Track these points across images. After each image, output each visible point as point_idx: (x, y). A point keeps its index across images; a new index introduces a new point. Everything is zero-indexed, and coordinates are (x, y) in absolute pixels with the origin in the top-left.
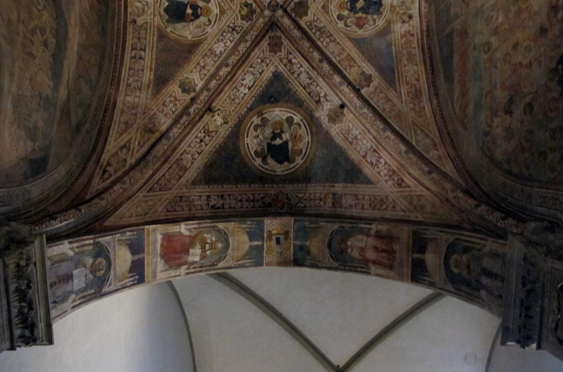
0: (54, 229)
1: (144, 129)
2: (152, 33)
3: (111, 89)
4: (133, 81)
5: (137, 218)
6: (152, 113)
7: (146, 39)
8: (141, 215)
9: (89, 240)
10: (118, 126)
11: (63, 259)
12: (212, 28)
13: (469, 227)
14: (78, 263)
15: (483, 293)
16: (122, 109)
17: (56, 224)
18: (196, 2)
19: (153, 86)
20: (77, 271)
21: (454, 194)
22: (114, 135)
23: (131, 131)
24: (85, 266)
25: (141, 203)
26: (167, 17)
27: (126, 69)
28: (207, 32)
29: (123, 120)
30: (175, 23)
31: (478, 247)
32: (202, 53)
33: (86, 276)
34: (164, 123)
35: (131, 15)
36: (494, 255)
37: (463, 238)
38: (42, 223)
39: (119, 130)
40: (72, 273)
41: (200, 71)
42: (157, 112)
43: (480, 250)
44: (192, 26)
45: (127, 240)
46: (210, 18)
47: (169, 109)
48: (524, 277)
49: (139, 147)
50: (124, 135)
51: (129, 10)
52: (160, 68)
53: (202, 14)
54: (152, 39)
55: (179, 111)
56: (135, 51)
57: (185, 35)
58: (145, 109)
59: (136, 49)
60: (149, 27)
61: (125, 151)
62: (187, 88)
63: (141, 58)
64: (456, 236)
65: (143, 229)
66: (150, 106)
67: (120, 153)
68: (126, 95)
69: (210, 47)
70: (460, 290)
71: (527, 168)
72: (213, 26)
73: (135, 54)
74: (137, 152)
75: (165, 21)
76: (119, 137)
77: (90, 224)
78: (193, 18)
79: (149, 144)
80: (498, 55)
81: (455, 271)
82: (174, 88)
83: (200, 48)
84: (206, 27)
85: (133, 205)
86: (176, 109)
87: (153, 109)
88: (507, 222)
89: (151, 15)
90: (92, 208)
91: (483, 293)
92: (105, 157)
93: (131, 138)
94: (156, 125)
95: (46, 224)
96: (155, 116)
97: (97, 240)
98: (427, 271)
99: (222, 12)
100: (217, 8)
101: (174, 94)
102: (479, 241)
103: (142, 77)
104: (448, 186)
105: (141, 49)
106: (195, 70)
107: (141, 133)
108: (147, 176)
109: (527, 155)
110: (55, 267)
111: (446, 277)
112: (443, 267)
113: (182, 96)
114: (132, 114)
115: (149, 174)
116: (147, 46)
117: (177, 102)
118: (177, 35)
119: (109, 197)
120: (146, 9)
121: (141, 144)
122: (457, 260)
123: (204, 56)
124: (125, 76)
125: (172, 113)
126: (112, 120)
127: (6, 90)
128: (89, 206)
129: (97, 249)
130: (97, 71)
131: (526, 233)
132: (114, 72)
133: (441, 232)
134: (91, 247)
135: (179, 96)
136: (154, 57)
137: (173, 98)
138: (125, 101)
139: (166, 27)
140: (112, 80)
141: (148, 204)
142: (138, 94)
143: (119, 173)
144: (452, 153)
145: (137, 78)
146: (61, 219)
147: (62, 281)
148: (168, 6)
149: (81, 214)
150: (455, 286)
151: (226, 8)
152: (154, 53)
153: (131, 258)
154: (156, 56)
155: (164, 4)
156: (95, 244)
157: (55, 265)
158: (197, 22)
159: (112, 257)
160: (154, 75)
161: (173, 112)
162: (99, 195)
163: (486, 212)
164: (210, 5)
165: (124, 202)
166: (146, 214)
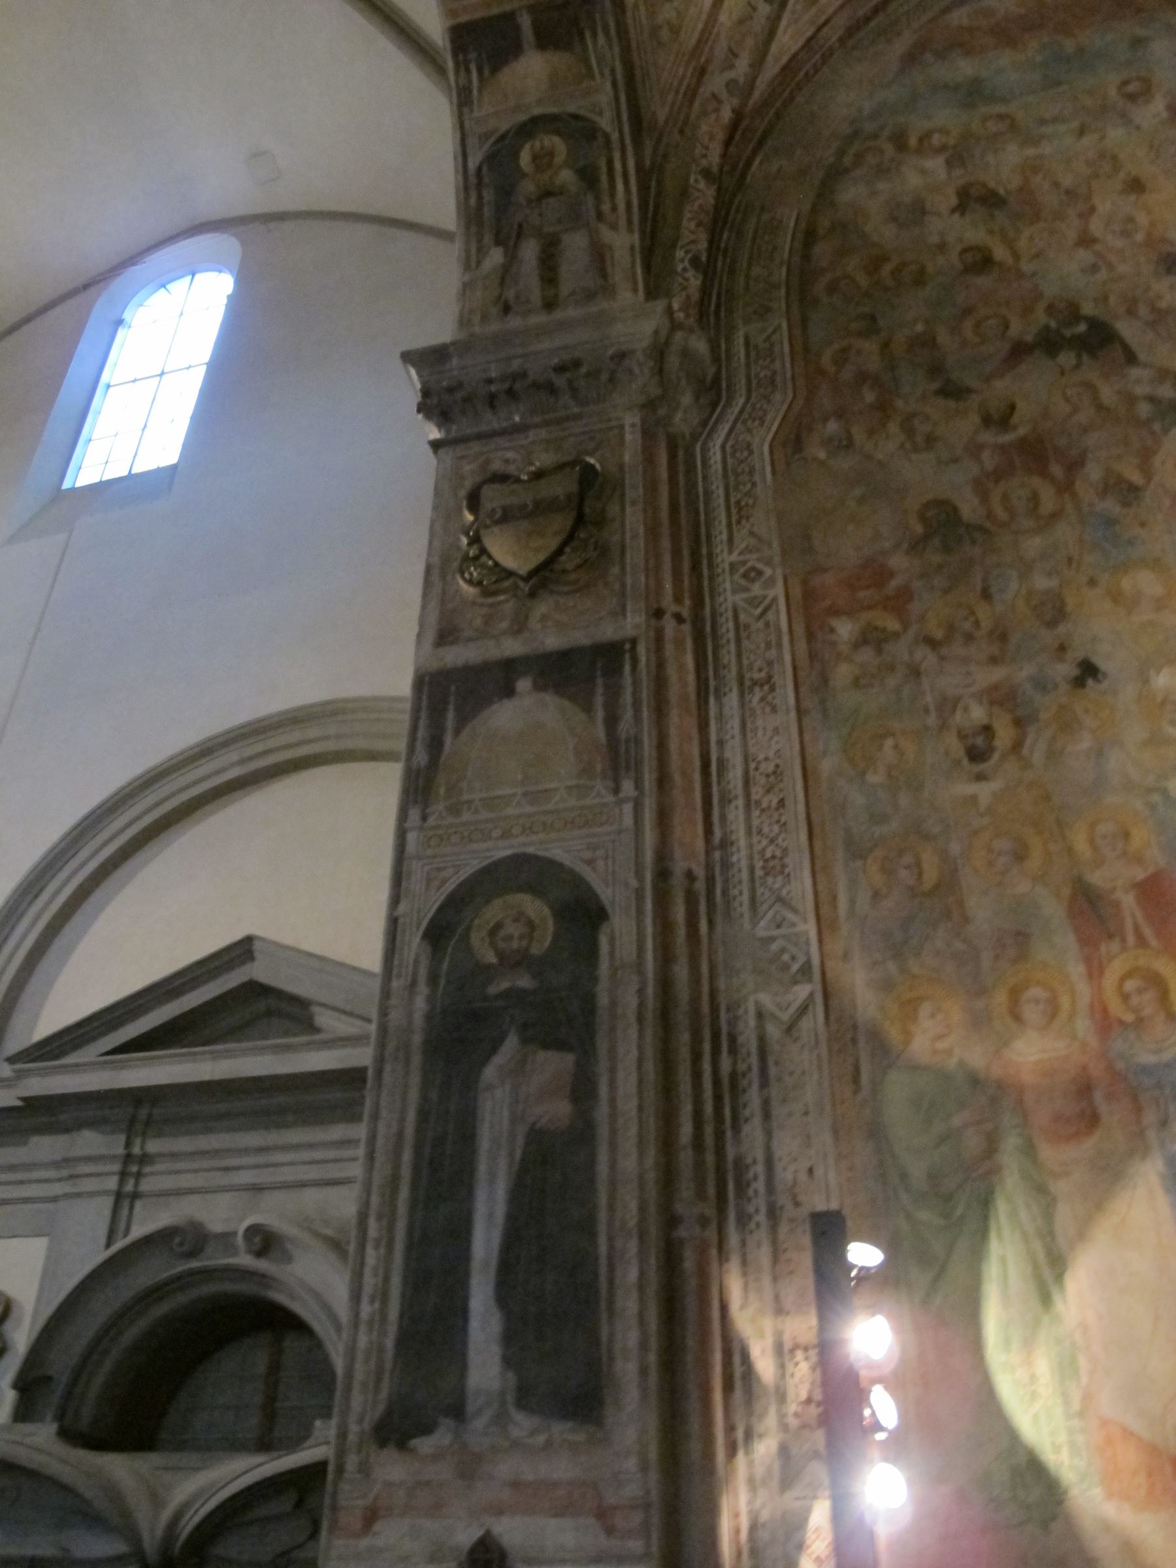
13: (648, 163)
15: (496, 256)
21: (724, 95)
31: (606, 207)
36: (600, 256)
37: (617, 156)
43: (600, 216)
48: (577, 364)
64: (615, 136)
70: (479, 185)
71: (832, 288)
80: (1115, 134)
81: (525, 158)
88: (690, 274)
91: (496, 256)
98: (495, 70)
102: (622, 207)
104: (742, 66)
109: (862, 280)
111: (497, 135)
112: (523, 117)
122: (551, 154)
131: (679, 336)
133: (614, 84)
144: (832, 35)
150: (485, 169)
163: (701, 206)
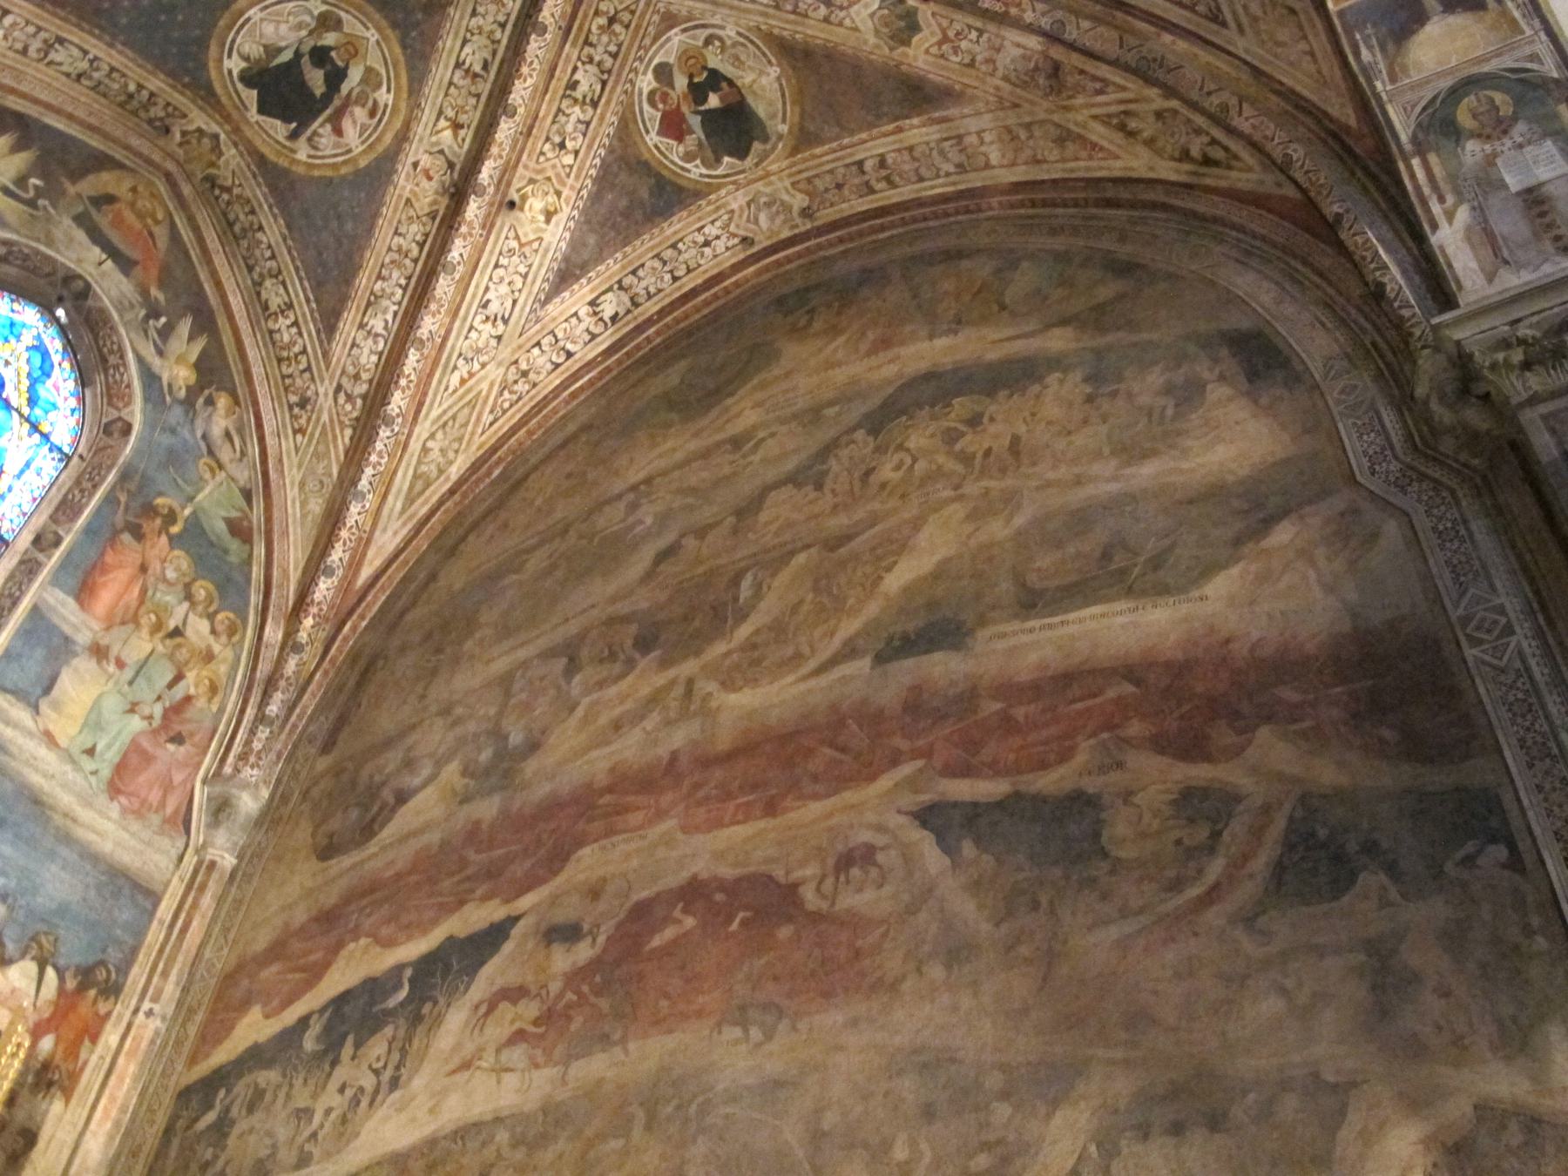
0: (1408, 279)
1: (1060, 92)
2: (811, 163)
3: (991, 208)
4: (948, 160)
5: (1310, 37)
6: (1007, 87)
7: (831, 172)
8: (1301, 28)
9: (1414, 174)
10: (1077, 159)
11: (1485, 237)
12: (722, 28)
14: (1488, 181)
16: (1026, 163)
17: (1393, 279)
18: (685, 96)
19: (936, 109)
20: (1508, 179)
22: (1103, 163)
23: (1076, 124)
24: (1490, 160)
25: (1265, 37)
26: (757, 146)
27: (925, 189)
28: (739, 34)
29: (1055, 152)
30: (760, 122)
32: (796, 23)
33: (1521, 146)
34: (1018, 45)
35: (797, 226)
38: (1401, 318)
39: (1084, 154)
40: (1518, 194)
41: (841, 8)
42: (1000, 73)
44: (745, 79)
45: (1383, 49)
46: (700, 44)
47: (977, 49)
49: (1111, 89)
50: (1094, 138)
51: (786, 234)
52: (885, 109)
53: (705, 68)
54: (825, 157)
55: (970, 20)
56: (873, 183)
57: (776, 85)
58: (1003, 109)
59: (867, 183)
60: (805, 175)
61: (1133, 124)
62: (903, 24)
63: (882, 163)
65: (1341, 14)
66: (991, 98)
67: (1145, 134)
68: (988, 166)
69: (771, 11)
72: (713, 26)
73: (878, 180)
74: (1124, 89)
75: (768, 147)
76: (1102, 149)
77: (1365, 169)
78: (724, 85)
79: (1090, 66)
82: (919, 56)
83: (785, 33)
84: (729, 42)
85: (1276, 56)
86: (970, 27)
87: (997, 88)
89: (771, 183)
90: (1322, 181)
92: (1168, 171)
93: (1095, 117)
94: (1032, 65)
95: (1400, 307)
96: (1013, 76)
97: (1408, 147)
99: (670, 20)
100: (669, 39)
101: (934, 50)
103: (927, 143)
105: (863, 173)
106: (847, 22)
107: (1070, 97)
108: (1182, 45)
110: (1511, 251)
113: (929, 26)
114: (1031, 137)
115: (1173, 43)
116: (848, 161)
117: (951, 34)
118: (784, 103)
119: (1276, 141)
120: (763, 200)
121: (1098, 85)
123: (799, 14)
124: (942, 186)
125: (986, 36)
126: (1065, 180)
127: (1113, 487)
128: (1319, 193)
129: (1432, 137)
130: (965, 264)
132: (947, 215)
134: (1433, 158)
135: (933, 34)
136: (864, 136)
137: (944, 47)
138: (1005, 162)
139: (780, 137)
140: (968, 211)
141: (1259, 13)
142: (972, 139)
143: (1200, 120)
145: (935, 153)
146: (1377, 269)
147: (1547, 220)
148: (731, 155)
149: (1347, 211)
151: (656, 18)
152: (856, 138)
153: (1435, 19)
154: (861, 130)
155: (732, 166)
156: (1421, 149)
157: (1506, 253)
158: (727, 69)
159: (1446, 84)
160: (907, 117)
161: (981, 32)
162: (1283, 168)
164: (671, 60)
165: (1277, 87)
166: (1292, 11)
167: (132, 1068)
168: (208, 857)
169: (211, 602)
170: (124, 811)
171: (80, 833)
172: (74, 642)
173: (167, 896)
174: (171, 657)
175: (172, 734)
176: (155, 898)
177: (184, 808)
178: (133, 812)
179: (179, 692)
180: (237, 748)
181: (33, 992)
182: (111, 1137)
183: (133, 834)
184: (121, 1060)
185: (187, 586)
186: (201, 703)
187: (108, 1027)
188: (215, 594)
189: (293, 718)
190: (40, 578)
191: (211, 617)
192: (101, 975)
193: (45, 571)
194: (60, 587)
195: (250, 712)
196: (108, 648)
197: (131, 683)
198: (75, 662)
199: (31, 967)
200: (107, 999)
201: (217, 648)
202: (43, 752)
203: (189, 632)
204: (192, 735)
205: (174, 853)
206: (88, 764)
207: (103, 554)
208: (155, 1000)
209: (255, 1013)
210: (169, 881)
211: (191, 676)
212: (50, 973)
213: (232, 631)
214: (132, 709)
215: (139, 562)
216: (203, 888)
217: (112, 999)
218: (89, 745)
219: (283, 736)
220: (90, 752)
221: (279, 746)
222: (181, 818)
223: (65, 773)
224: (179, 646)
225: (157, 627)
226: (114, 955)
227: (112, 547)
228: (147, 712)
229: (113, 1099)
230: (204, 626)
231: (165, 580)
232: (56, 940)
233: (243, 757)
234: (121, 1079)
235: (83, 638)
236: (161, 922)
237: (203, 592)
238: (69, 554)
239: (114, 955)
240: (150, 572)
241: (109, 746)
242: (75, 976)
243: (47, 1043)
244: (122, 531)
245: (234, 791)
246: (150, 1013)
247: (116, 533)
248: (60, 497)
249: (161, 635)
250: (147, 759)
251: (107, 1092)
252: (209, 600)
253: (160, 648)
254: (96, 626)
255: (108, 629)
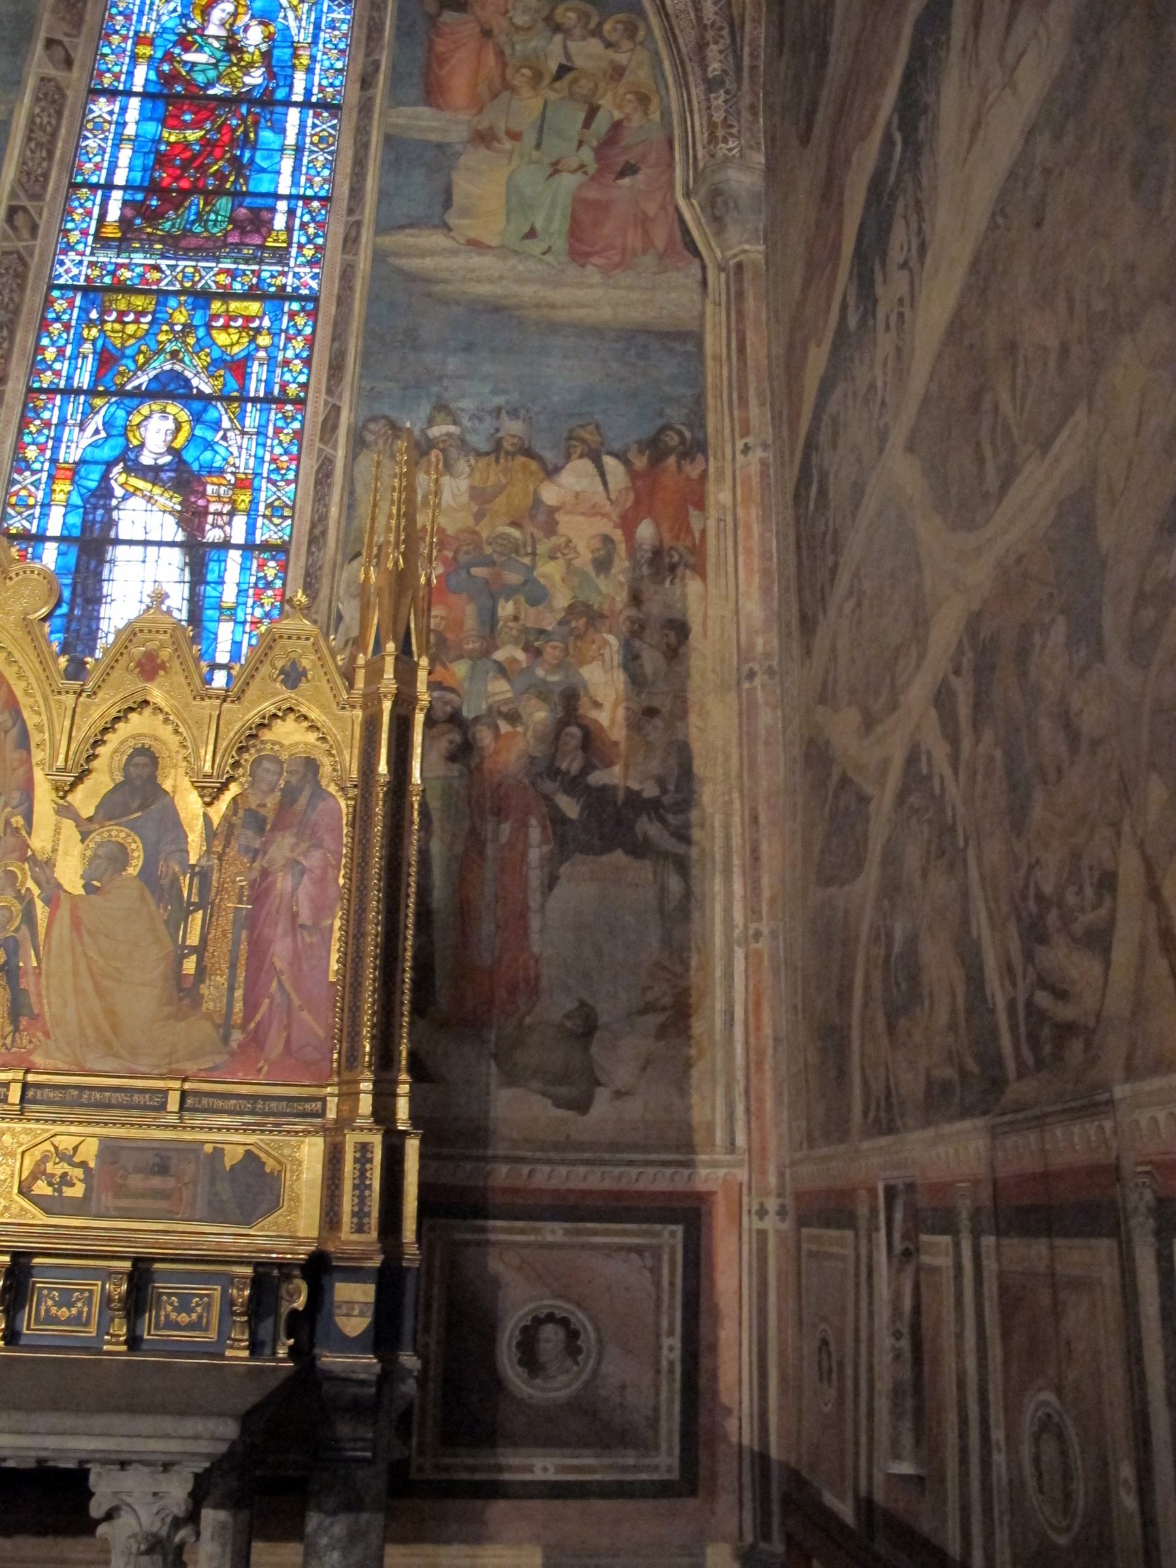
167: (754, 512)
168: (732, 263)
169: (588, 17)
170: (605, 271)
171: (561, 315)
172: (448, 144)
173: (709, 327)
174: (572, 96)
175: (619, 168)
176: (698, 339)
177: (678, 235)
178: (617, 266)
179: (601, 124)
180: (702, 137)
181: (601, 488)
182: (766, 590)
183: (629, 288)
184: (740, 512)
185: (548, 19)
186: (637, 120)
187: (711, 487)
188: (589, 8)
189: (746, 61)
190: (377, 110)
191: (597, 32)
192: (673, 439)
193: (378, 101)
194: (405, 104)
195: (697, 91)
196: (491, 128)
197: (538, 146)
198: (462, 160)
199: (586, 465)
200: (693, 460)
201: (622, 58)
202: (476, 260)
203: (579, 62)
204: (644, 157)
205: (693, 282)
206: (536, 247)
207: (430, 49)
208: (745, 432)
209: (813, 352)
210: (702, 315)
211: (606, 102)
212: (609, 461)
213: (631, 31)
214: (556, 169)
215: (478, 29)
216: (740, 295)
217: (700, 457)
218: (526, 229)
219: (746, 86)
220: (532, 234)
221: (746, 100)
222: (680, 246)
223: (514, 267)
224: (575, 81)
225: (537, 76)
226: (676, 415)
227: (439, 35)
228: (574, 163)
229: (749, 551)
230: (594, 45)
231: (519, 29)
232: (598, 427)
233: (712, 139)
234: (748, 528)
235: (457, 134)
236: (717, 358)
237: (571, 15)
238: (394, 68)
239: (676, 415)
240: (496, 31)
241: (549, 219)
242: (641, 452)
243: (645, 531)
244: (439, 15)
245: (717, 178)
246: (746, 449)
247: (432, 19)
248: (365, 31)
249: (547, 81)
250: (601, 208)
251: (740, 549)
252: (585, 17)
253: (553, 96)
254: (464, 116)
255: (480, 111)
